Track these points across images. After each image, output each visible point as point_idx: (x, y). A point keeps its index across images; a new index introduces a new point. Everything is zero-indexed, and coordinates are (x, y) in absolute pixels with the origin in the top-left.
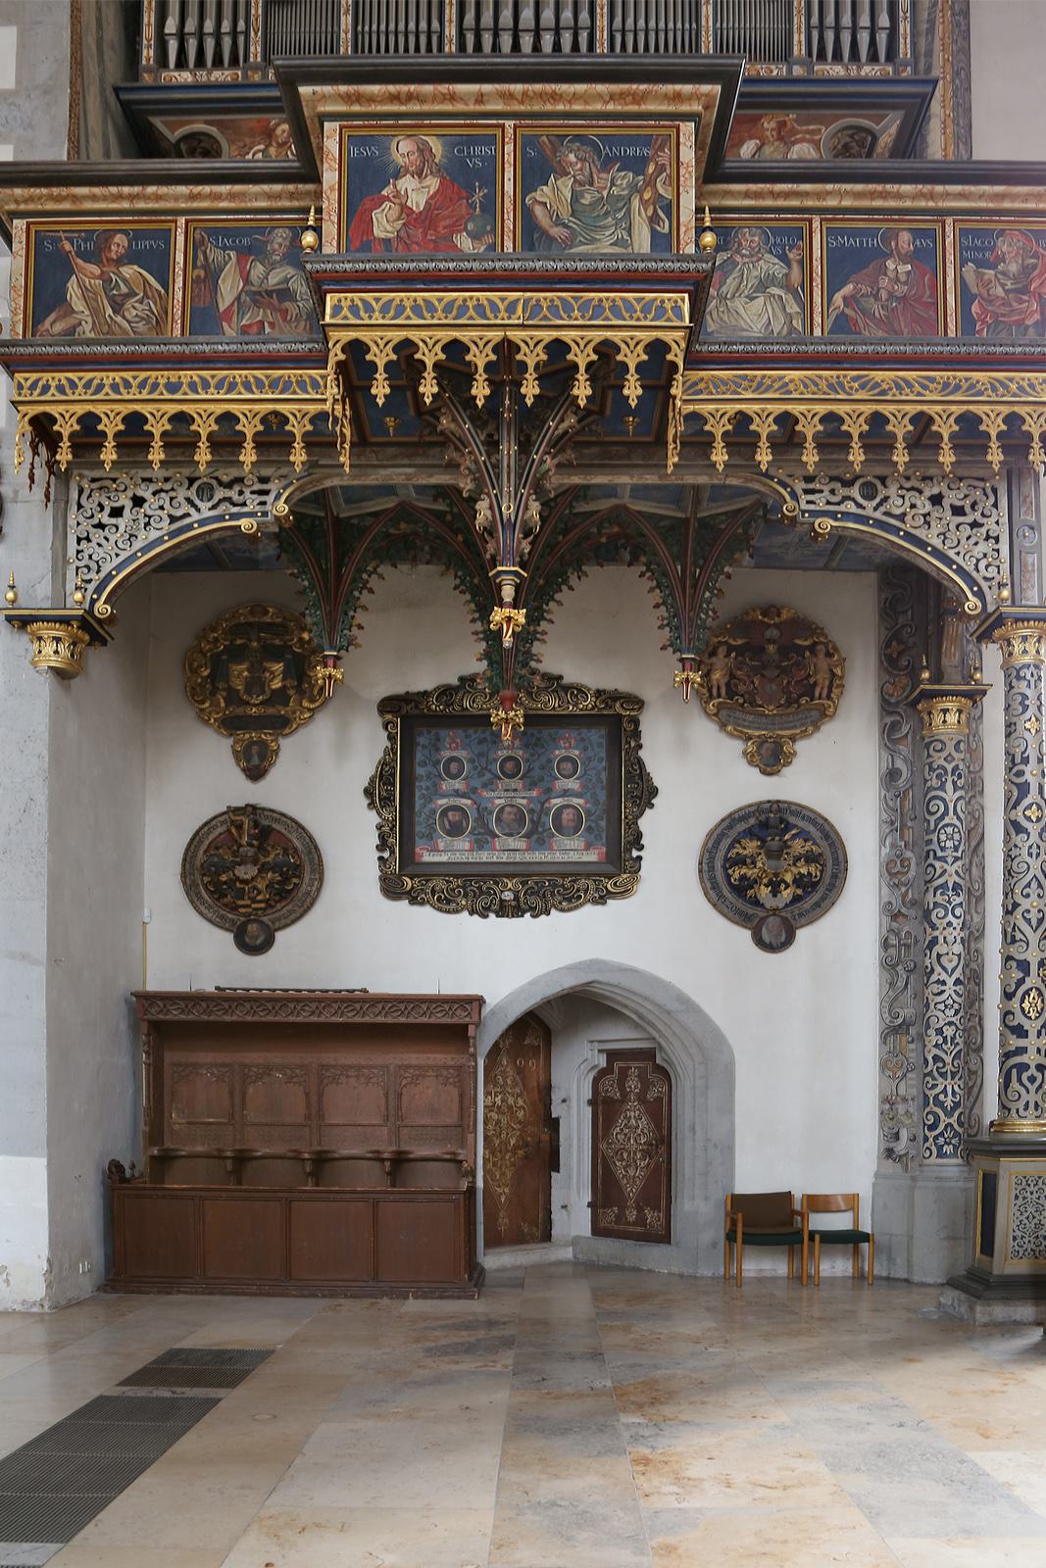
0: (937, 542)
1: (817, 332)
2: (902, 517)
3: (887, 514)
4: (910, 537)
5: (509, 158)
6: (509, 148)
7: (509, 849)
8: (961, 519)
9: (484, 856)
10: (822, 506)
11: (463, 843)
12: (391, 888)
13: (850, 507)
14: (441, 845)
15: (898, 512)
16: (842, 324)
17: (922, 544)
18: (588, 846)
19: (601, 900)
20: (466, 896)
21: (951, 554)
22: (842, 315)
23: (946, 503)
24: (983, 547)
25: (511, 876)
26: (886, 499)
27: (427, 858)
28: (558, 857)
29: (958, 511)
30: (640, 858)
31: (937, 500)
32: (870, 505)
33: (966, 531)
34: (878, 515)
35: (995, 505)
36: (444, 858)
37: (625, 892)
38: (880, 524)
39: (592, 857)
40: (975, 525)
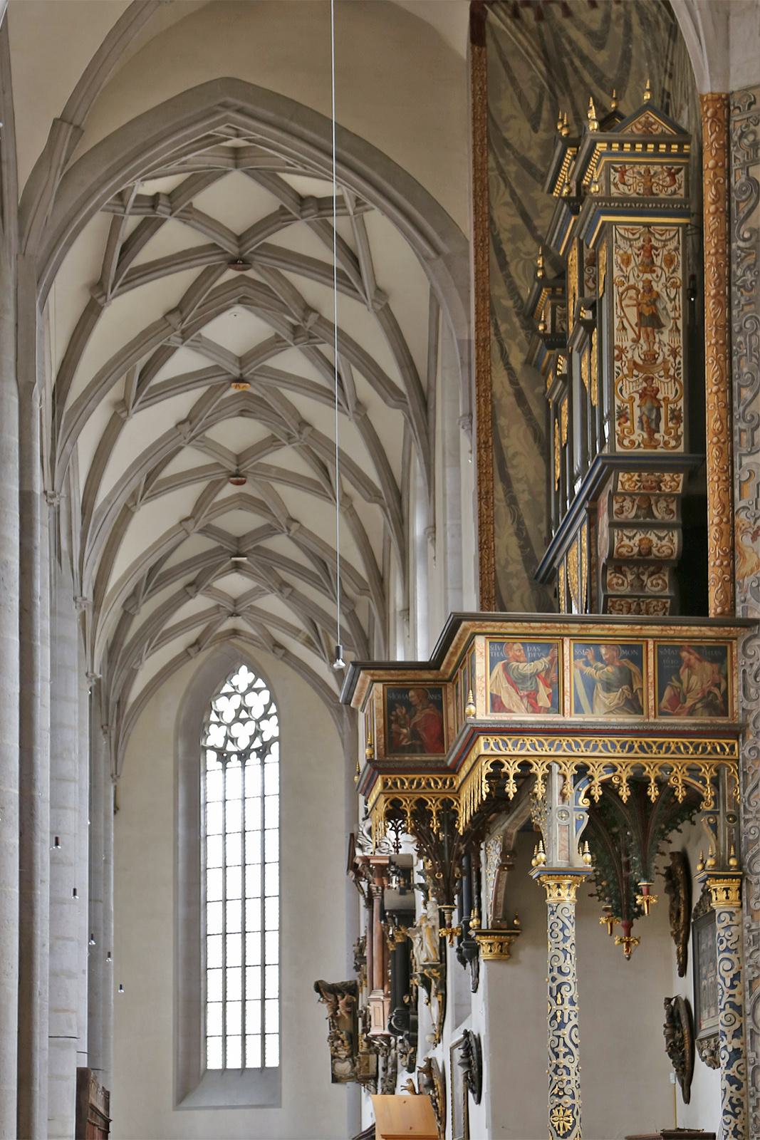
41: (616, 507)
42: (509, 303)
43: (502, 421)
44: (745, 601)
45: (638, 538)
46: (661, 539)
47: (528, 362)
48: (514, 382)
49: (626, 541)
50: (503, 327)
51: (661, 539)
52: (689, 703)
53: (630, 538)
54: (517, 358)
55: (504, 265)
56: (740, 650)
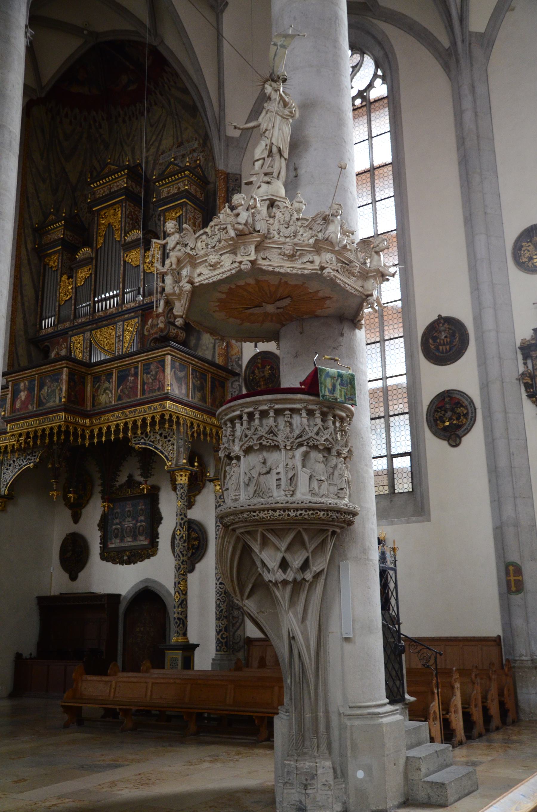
0: (160, 448)
1: (113, 403)
2: (153, 442)
3: (150, 441)
4: (155, 448)
5: (36, 385)
6: (36, 382)
7: (129, 542)
8: (166, 440)
9: (123, 545)
10: (137, 442)
11: (118, 541)
12: (103, 557)
13: (142, 441)
14: (113, 541)
15: (152, 440)
16: (120, 398)
17: (157, 449)
18: (146, 539)
19: (148, 557)
20: (118, 558)
21: (163, 451)
22: (120, 396)
23: (163, 435)
24: (171, 448)
25: (128, 551)
26: (150, 437)
27: (111, 546)
28: (139, 543)
29: (166, 437)
30: (158, 542)
31: (161, 435)
32: (146, 439)
33: (167, 443)
34: (148, 442)
35: (174, 434)
36: (113, 546)
37: (154, 554)
38: (150, 445)
39: (146, 543)
40: (169, 441)
41: (169, 315)
42: (29, 222)
43: (23, 269)
44: (232, 365)
45: (176, 330)
46: (181, 333)
47: (34, 249)
48: (28, 255)
49: (173, 331)
50: (26, 231)
51: (181, 333)
52: (217, 403)
53: (174, 330)
54: (30, 246)
55: (29, 207)
56: (230, 385)
